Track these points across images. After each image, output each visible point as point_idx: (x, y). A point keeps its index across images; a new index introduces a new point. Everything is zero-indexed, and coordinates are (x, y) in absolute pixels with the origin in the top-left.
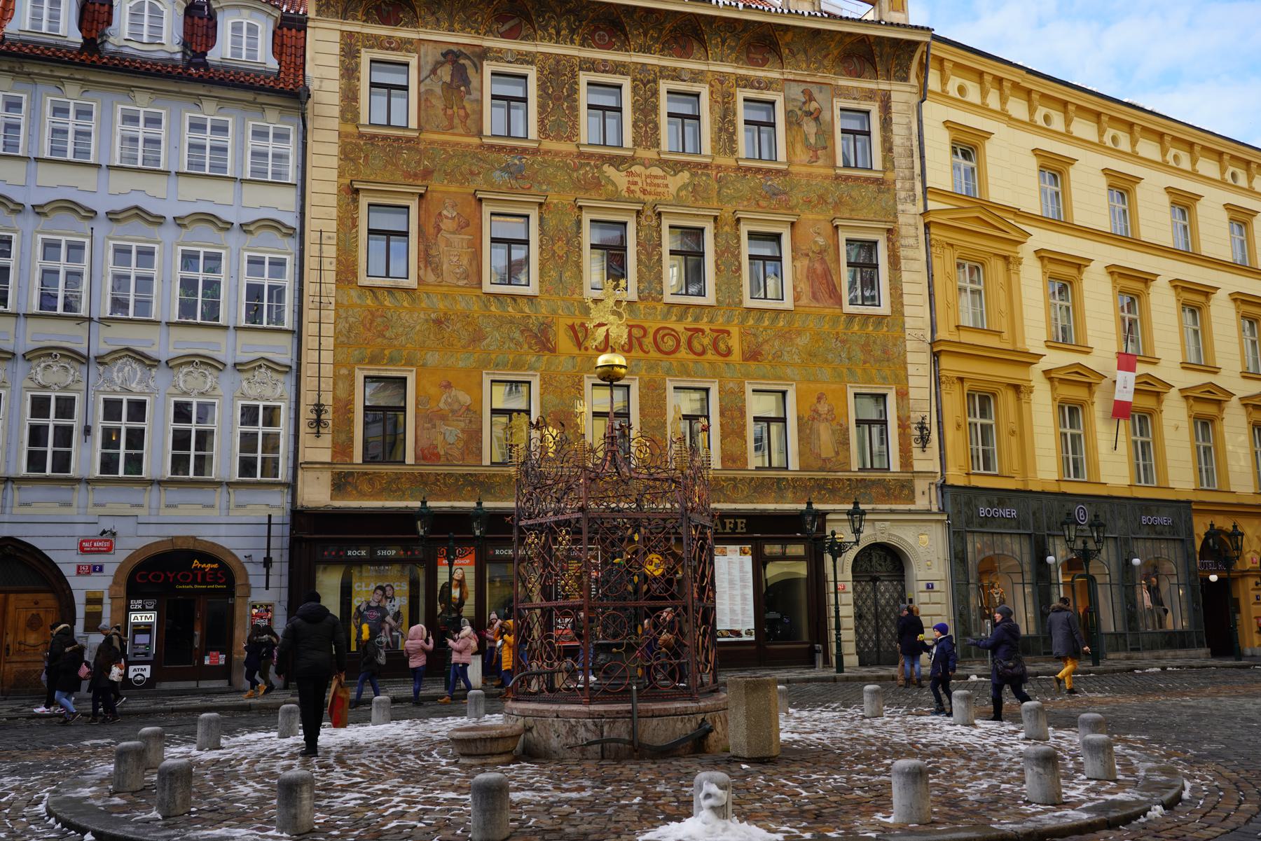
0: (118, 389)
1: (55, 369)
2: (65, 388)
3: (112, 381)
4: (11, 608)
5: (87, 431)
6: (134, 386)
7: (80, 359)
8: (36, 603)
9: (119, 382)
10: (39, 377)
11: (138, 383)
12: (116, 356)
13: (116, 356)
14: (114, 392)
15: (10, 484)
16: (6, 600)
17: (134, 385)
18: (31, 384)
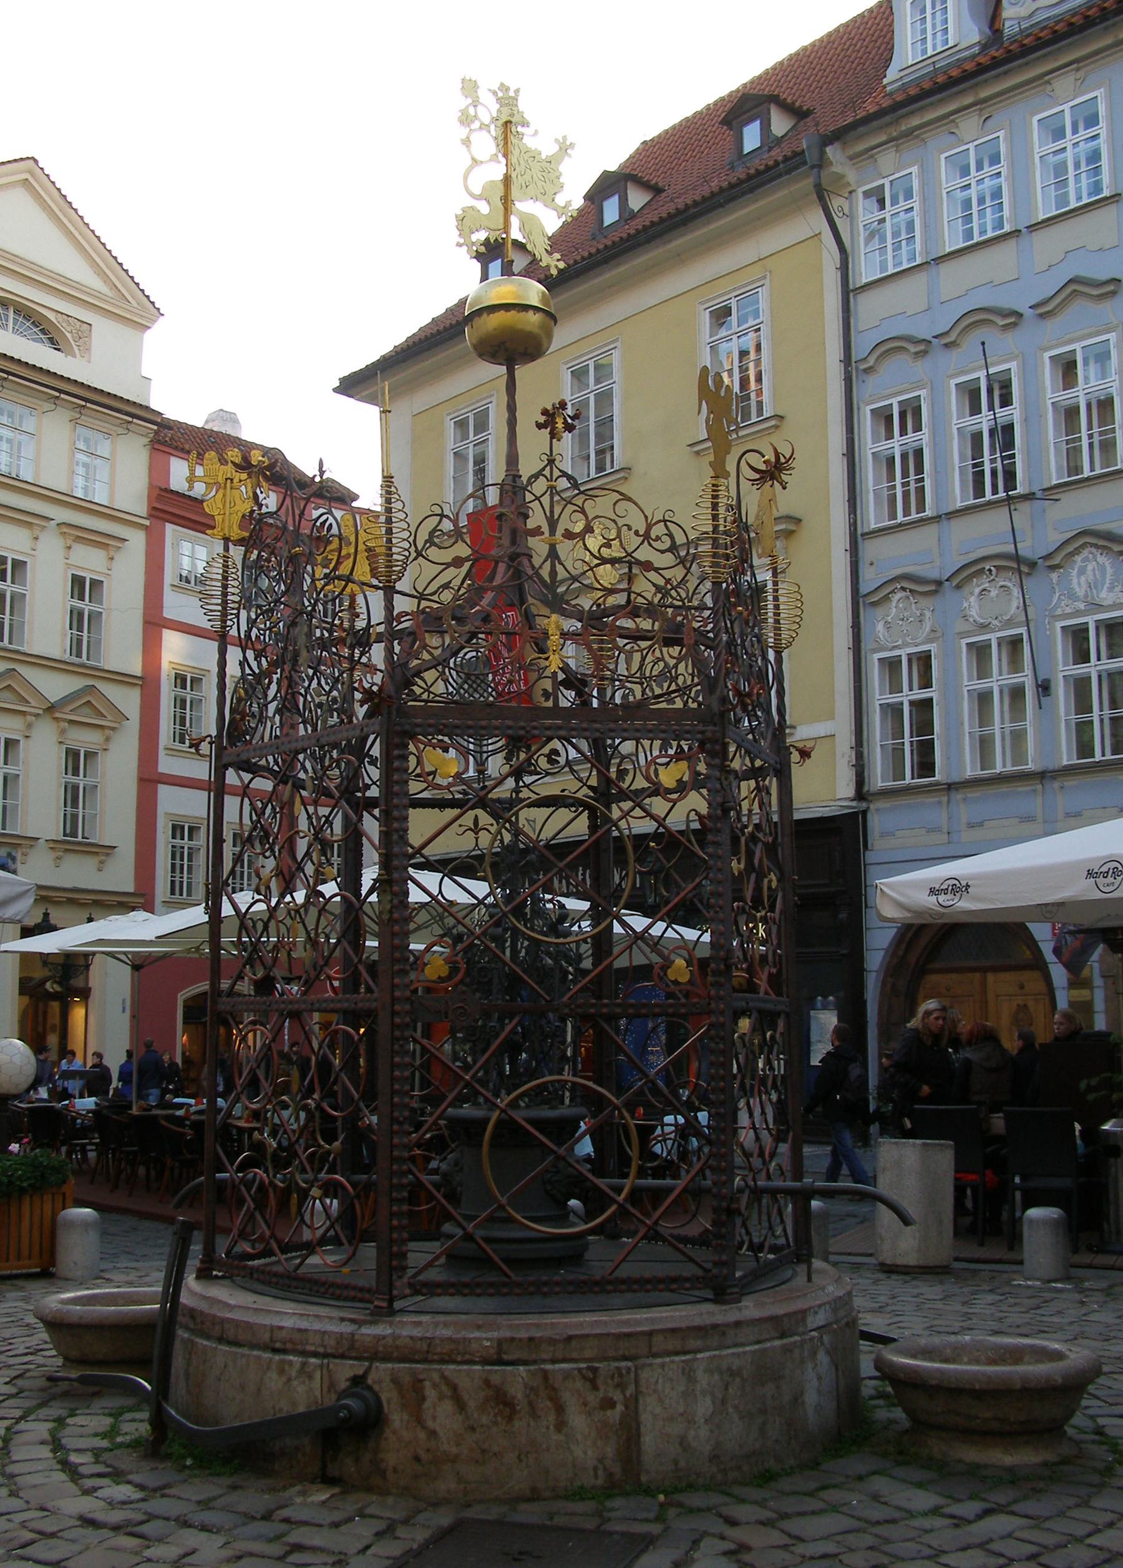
0: (1082, 606)
1: (993, 593)
2: (1009, 623)
3: (1072, 596)
4: (990, 996)
5: (1044, 688)
6: (1106, 596)
7: (1020, 565)
8: (1022, 987)
9: (1081, 593)
10: (974, 613)
11: (1111, 589)
12: (1070, 548)
13: (1070, 548)
14: (1077, 613)
15: (957, 796)
16: (984, 983)
17: (1103, 594)
18: (967, 627)
